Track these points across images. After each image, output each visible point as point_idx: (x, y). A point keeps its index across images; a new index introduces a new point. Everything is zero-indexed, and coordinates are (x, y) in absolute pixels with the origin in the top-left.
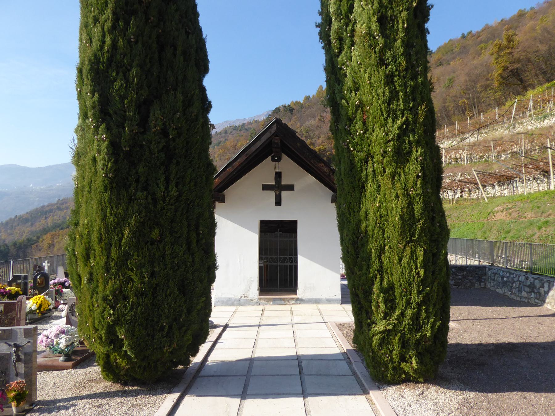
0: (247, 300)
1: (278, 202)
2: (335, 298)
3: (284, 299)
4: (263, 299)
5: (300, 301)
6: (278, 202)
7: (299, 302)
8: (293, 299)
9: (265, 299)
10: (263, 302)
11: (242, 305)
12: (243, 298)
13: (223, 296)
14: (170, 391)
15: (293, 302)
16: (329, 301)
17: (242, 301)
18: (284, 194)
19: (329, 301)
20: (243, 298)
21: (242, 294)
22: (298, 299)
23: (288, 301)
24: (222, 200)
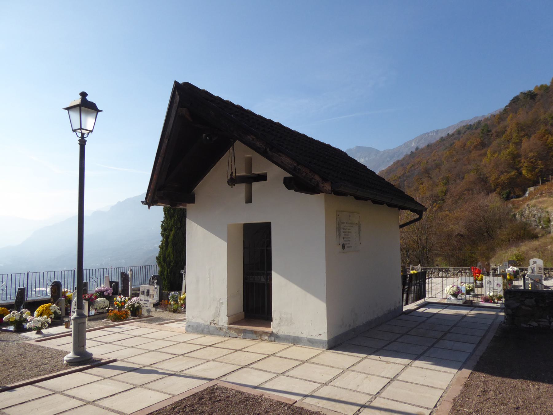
0: (217, 329)
1: (249, 200)
2: (319, 338)
3: (255, 332)
4: (233, 328)
5: (274, 337)
6: (249, 200)
7: (273, 338)
8: (266, 333)
9: (235, 330)
10: (232, 333)
11: (212, 334)
12: (213, 325)
13: (193, 321)
14: (297, 408)
15: (266, 338)
16: (312, 342)
17: (211, 329)
18: (256, 186)
19: (312, 342)
20: (213, 325)
21: (211, 320)
22: (272, 334)
23: (261, 335)
24: (192, 200)
